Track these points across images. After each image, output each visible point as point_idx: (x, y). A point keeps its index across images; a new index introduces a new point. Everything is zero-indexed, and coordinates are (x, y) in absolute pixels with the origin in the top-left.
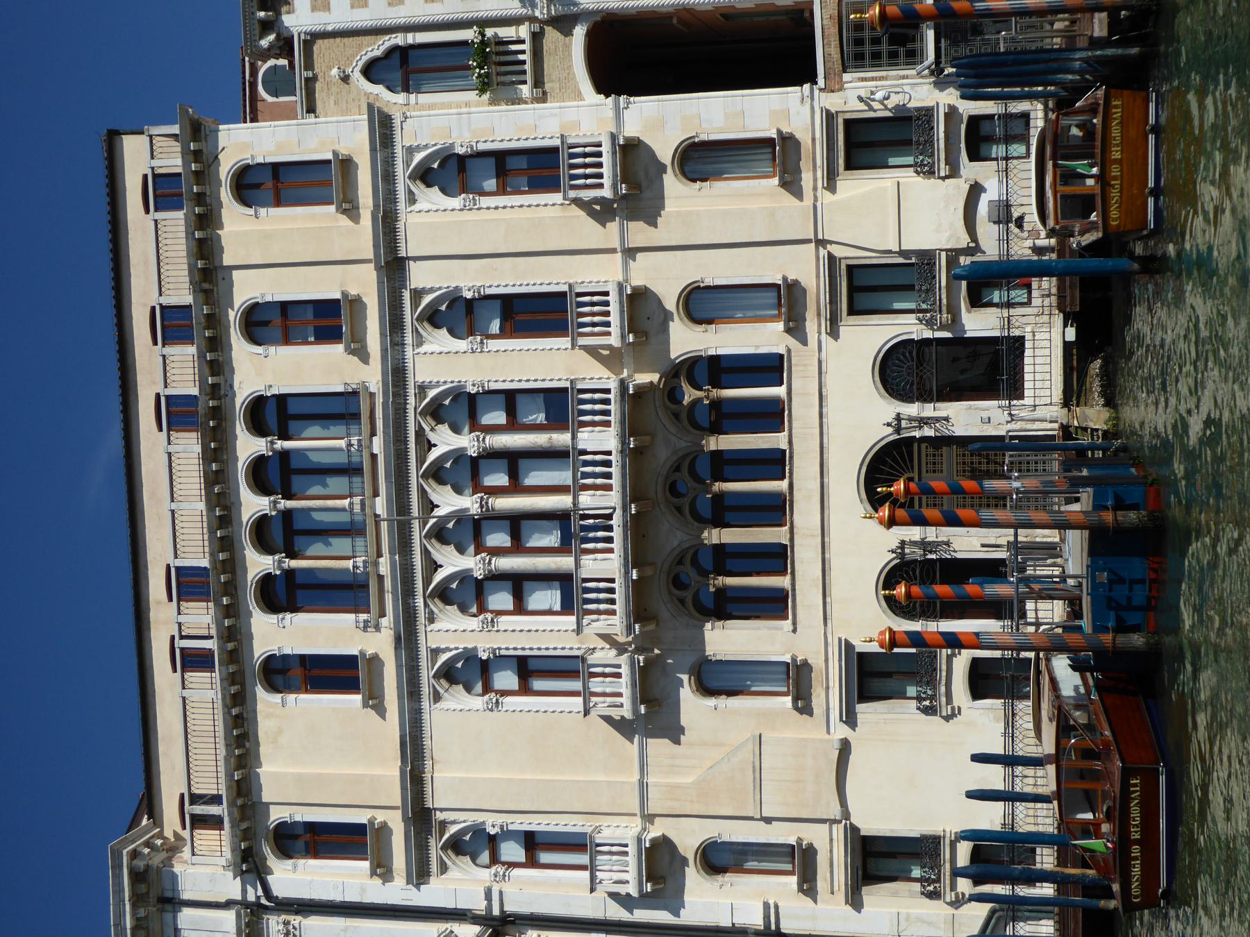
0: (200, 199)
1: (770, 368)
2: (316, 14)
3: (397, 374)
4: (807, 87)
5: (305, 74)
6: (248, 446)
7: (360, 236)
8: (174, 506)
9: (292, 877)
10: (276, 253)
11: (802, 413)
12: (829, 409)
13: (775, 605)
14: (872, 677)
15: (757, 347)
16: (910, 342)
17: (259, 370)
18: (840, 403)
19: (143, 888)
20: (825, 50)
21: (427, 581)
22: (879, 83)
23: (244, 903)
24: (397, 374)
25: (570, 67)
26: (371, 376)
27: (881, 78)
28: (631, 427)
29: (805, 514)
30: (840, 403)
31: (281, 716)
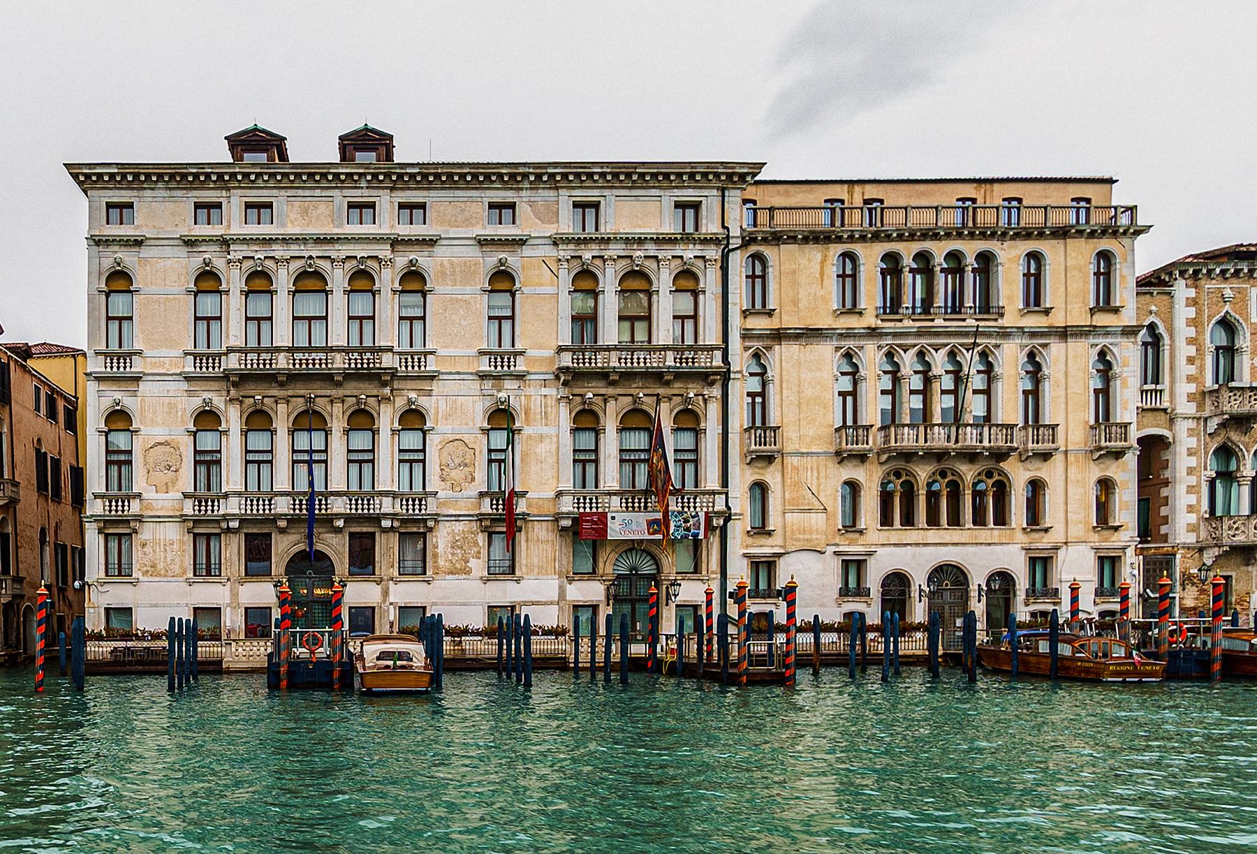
1: (1001, 519)
3: (1005, 334)
7: (1080, 318)
9: (738, 262)
11: (982, 535)
12: (983, 547)
13: (886, 520)
14: (854, 566)
17: (1010, 259)
18: (987, 553)
21: (899, 346)
24: (1005, 334)
26: (1008, 321)
30: (987, 553)
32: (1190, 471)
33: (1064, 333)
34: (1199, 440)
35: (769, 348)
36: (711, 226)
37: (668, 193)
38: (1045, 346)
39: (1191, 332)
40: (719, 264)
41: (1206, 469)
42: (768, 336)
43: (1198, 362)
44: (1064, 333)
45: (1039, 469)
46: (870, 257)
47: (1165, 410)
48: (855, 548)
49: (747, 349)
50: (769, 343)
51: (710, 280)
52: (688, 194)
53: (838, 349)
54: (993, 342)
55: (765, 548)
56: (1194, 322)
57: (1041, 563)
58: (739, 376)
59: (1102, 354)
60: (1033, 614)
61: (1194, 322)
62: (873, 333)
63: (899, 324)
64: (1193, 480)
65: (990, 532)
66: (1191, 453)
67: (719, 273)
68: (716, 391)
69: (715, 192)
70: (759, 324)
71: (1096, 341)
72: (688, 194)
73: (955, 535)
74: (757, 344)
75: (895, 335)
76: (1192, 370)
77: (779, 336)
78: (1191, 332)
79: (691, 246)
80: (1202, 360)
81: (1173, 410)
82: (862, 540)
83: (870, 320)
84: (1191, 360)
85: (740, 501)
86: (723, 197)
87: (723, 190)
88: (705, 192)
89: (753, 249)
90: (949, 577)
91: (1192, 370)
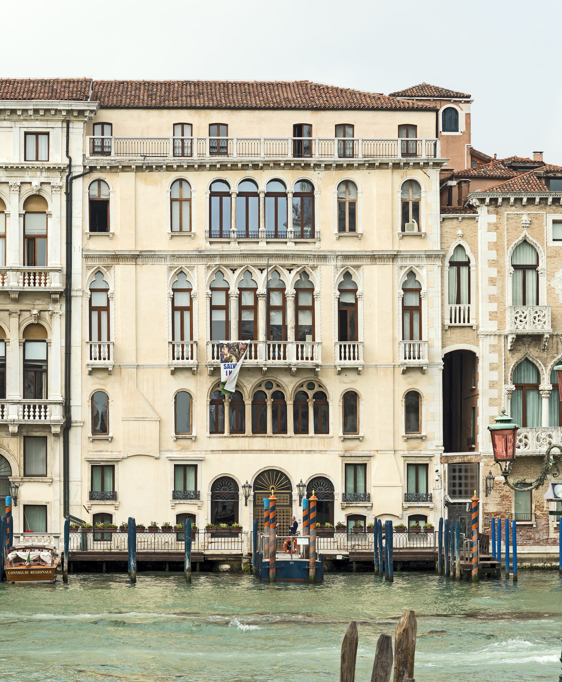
0: (407, 164)
1: (322, 427)
2: (487, 225)
3: (324, 257)
4: (443, 448)
5: (460, 218)
6: (291, 179)
8: (262, 141)
10: (377, 196)
13: (216, 428)
14: (184, 470)
15: (332, 423)
16: (333, 489)
18: (306, 458)
19: (75, 114)
20: (458, 456)
21: (227, 266)
22: (443, 479)
23: (70, 166)
24: (324, 257)
25: (457, 343)
27: (445, 480)
28: (300, 370)
29: (259, 442)
30: (306, 458)
31: (159, 187)
32: (493, 385)
33: (374, 258)
34: (500, 356)
35: (108, 267)
36: (58, 158)
37: (18, 124)
38: (357, 267)
39: (493, 255)
40: (64, 190)
41: (506, 382)
42: (108, 257)
43: (499, 283)
44: (374, 258)
45: (353, 382)
46: (200, 184)
47: (472, 327)
48: (186, 455)
49: (89, 268)
50: (108, 262)
51: (56, 203)
52: (37, 126)
53: (171, 268)
54: (311, 263)
55: (104, 452)
56: (496, 246)
57: (356, 469)
58: (80, 294)
59: (411, 274)
60: (350, 518)
61: (496, 246)
62: (201, 256)
63: (226, 246)
64: (494, 393)
65: (310, 439)
66: (493, 368)
67: (64, 197)
68: (60, 308)
69: (59, 124)
70: (100, 244)
71: (404, 263)
72: (37, 126)
73: (277, 442)
74: (97, 263)
75: (222, 256)
76: (494, 290)
77: (117, 257)
78: (493, 255)
79: (39, 173)
80: (503, 281)
81: (478, 327)
82: (194, 446)
83: (201, 242)
84: (492, 281)
85: (82, 412)
86: (68, 128)
87: (68, 122)
88: (51, 124)
89: (96, 175)
90: (272, 480)
91: (494, 290)
